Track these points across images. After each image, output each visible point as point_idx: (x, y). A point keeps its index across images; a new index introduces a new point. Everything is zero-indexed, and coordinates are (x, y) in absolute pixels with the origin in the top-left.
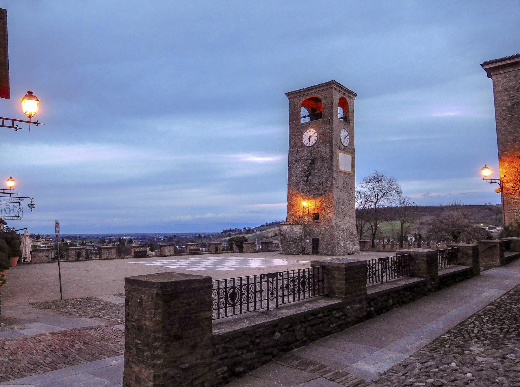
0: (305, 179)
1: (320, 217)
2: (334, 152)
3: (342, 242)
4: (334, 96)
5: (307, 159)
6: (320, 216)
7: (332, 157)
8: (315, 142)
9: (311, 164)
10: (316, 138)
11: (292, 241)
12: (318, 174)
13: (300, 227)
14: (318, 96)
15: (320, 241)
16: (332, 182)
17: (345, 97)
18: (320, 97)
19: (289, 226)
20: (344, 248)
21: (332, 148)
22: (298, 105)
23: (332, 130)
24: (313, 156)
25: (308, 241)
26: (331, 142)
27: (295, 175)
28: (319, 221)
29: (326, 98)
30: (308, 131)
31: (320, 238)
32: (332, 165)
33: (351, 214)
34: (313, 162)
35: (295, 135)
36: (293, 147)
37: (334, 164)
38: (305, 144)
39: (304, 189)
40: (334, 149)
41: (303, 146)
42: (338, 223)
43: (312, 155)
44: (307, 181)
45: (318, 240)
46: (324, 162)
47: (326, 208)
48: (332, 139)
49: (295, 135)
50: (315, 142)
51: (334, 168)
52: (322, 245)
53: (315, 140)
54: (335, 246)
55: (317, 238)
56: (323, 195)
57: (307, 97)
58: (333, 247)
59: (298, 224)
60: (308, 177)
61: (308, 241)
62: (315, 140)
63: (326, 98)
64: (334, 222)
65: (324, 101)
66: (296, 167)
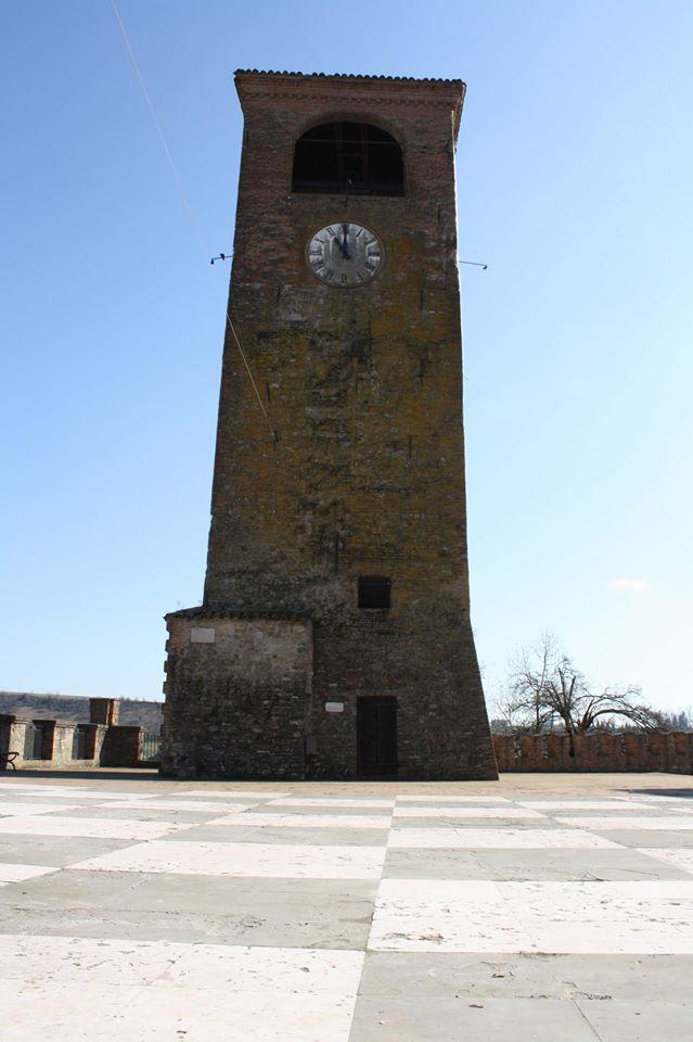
15: (405, 710)
19: (229, 627)
25: (334, 707)
28: (394, 611)
34: (361, 350)
38: (320, 272)
49: (266, 231)
55: (387, 692)
61: (334, 707)
62: (368, 265)
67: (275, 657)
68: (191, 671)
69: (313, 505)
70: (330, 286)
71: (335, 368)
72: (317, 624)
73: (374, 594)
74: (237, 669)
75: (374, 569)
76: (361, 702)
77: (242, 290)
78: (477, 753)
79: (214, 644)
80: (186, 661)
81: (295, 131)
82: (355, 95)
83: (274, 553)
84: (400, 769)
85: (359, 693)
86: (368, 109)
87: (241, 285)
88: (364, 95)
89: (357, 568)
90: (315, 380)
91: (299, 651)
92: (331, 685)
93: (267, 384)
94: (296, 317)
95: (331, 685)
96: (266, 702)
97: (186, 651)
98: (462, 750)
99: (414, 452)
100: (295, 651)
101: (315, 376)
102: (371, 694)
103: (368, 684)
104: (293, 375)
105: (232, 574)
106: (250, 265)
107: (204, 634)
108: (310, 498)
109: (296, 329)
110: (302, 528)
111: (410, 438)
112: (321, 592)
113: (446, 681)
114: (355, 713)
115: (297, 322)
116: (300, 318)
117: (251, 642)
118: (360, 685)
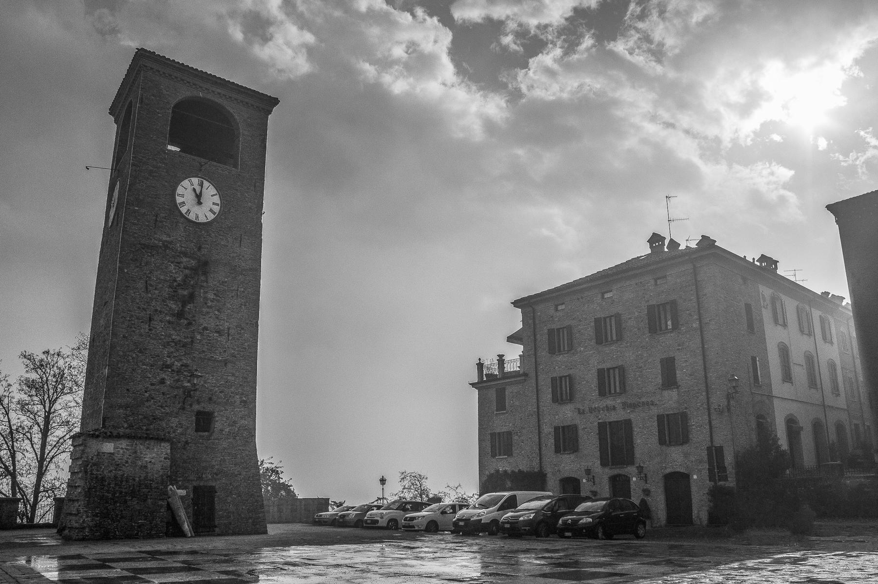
0: (174, 306)
5: (185, 254)
6: (218, 424)
9: (194, 270)
10: (217, 209)
13: (166, 448)
14: (229, 109)
19: (124, 444)
24: (204, 251)
27: (140, 285)
28: (215, 436)
38: (183, 210)
39: (170, 336)
43: (200, 249)
44: (180, 315)
45: (212, 491)
50: (211, 217)
56: (229, 366)
59: (160, 439)
60: (184, 306)
62: (211, 210)
68: (98, 471)
69: (168, 367)
71: (186, 276)
72: (172, 444)
73: (204, 421)
74: (127, 470)
76: (196, 489)
77: (135, 211)
79: (113, 454)
80: (94, 464)
81: (173, 102)
82: (214, 89)
83: (147, 395)
84: (217, 530)
85: (195, 484)
86: (219, 100)
88: (219, 91)
89: (196, 407)
90: (175, 284)
91: (165, 458)
94: (165, 238)
97: (95, 458)
98: (250, 518)
101: (175, 281)
102: (202, 484)
104: (162, 277)
105: (121, 407)
107: (108, 447)
109: (166, 246)
110: (162, 381)
111: (229, 329)
112: (174, 422)
114: (192, 496)
115: (166, 241)
117: (135, 452)
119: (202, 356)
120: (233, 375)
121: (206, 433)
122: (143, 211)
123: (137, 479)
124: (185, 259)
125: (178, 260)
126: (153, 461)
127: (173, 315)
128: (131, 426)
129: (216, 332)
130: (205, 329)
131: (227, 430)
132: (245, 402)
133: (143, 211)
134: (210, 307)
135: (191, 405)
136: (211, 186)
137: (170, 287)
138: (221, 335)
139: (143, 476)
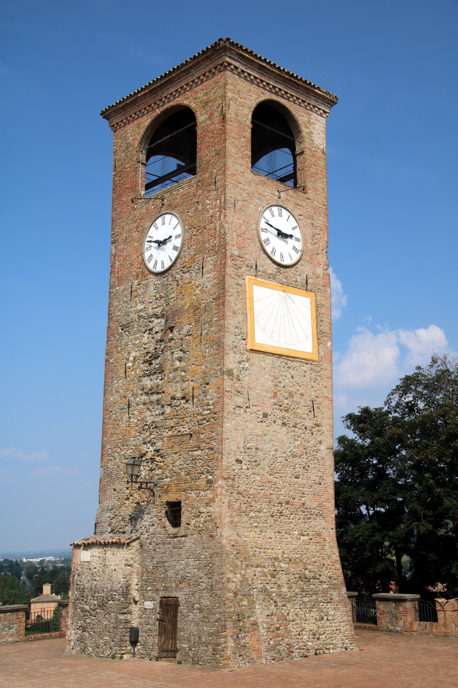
1: (184, 519)
2: (229, 281)
3: (260, 613)
4: (229, 95)
7: (220, 298)
8: (176, 253)
11: (102, 605)
12: (183, 364)
14: (186, 102)
15: (182, 609)
16: (220, 390)
17: (283, 101)
18: (193, 105)
20: (274, 631)
21: (221, 268)
22: (136, 143)
23: (222, 208)
25: (149, 605)
26: (221, 249)
28: (182, 530)
29: (206, 103)
30: (159, 222)
31: (181, 596)
32: (222, 328)
33: (311, 503)
35: (125, 241)
36: (120, 280)
37: (231, 322)
40: (229, 270)
41: (145, 272)
42: (250, 537)
46: (197, 321)
47: (202, 482)
48: (223, 236)
51: (229, 340)
52: (189, 624)
53: (175, 248)
54: (224, 627)
55: (174, 594)
56: (194, 437)
57: (158, 112)
58: (217, 634)
61: (149, 605)
62: (175, 248)
63: (206, 103)
64: (226, 534)
65: (201, 118)
66: (127, 345)
67: (115, 570)
68: (80, 581)
70: (157, 274)
75: (172, 497)
78: (218, 645)
85: (161, 594)
87: (114, 291)
89: (165, 498)
92: (149, 588)
93: (125, 364)
94: (140, 307)
95: (149, 588)
96: (110, 602)
99: (195, 400)
100: (123, 566)
103: (166, 589)
104: (138, 354)
106: (118, 273)
108: (144, 448)
113: (204, 585)
114: (158, 610)
115: (141, 311)
116: (142, 307)
118: (162, 588)
119: (170, 433)
120: (199, 448)
121: (176, 530)
122: (122, 287)
123: (105, 589)
124: (156, 321)
125: (151, 325)
126: (116, 568)
127: (147, 394)
128: (112, 531)
129: (183, 398)
130: (173, 398)
131: (193, 522)
132: (209, 482)
133: (122, 287)
134: (176, 370)
135: (160, 497)
136: (174, 218)
137: (145, 362)
138: (187, 401)
139: (109, 586)
